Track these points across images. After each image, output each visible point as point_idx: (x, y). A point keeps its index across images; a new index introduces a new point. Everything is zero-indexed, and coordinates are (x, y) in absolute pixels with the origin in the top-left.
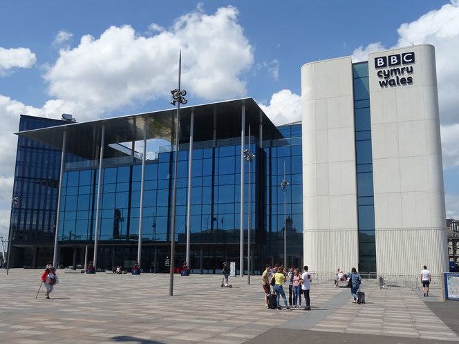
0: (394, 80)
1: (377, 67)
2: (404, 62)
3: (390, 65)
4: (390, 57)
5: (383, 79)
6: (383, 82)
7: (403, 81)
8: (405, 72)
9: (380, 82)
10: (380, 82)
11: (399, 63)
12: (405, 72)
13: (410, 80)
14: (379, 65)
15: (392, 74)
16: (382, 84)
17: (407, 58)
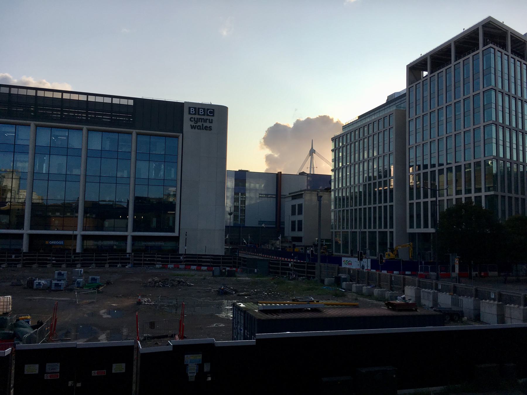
0: (200, 126)
1: (190, 113)
2: (208, 115)
3: (199, 114)
4: (199, 109)
5: (193, 124)
6: (193, 125)
7: (206, 128)
8: (208, 121)
9: (191, 125)
10: (191, 125)
11: (204, 115)
12: (208, 121)
13: (210, 128)
14: (191, 113)
15: (199, 122)
16: (192, 127)
17: (210, 112)
